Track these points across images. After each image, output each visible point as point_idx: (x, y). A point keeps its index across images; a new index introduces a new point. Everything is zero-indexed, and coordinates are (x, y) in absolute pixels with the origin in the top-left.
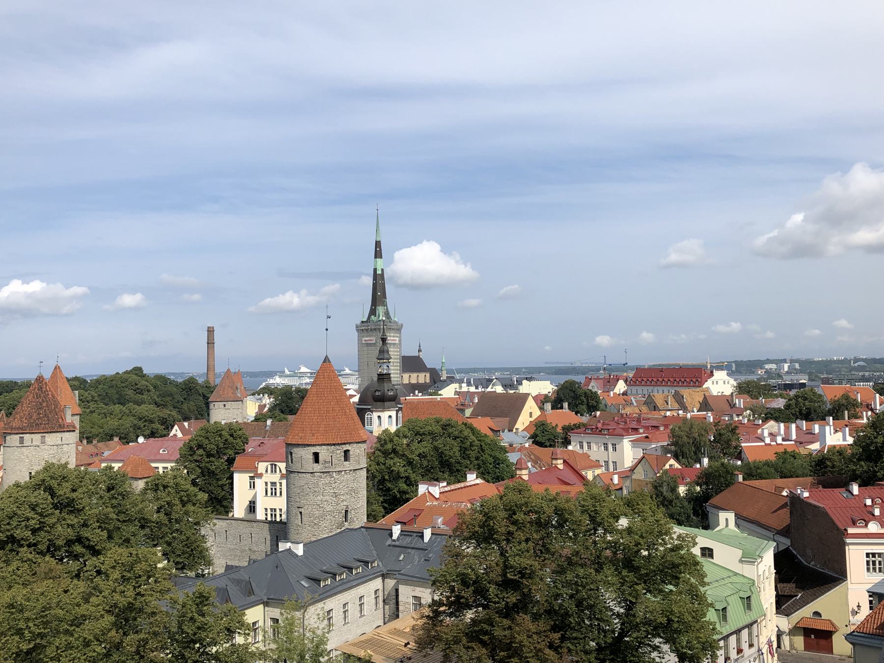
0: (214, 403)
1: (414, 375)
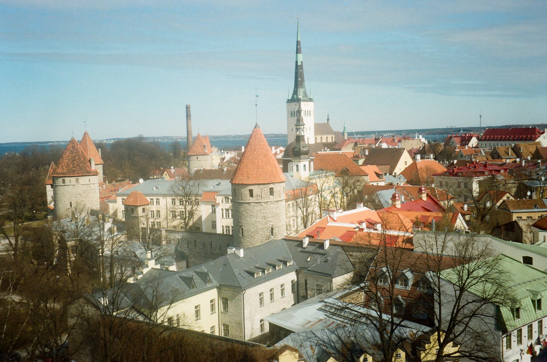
1: (324, 137)
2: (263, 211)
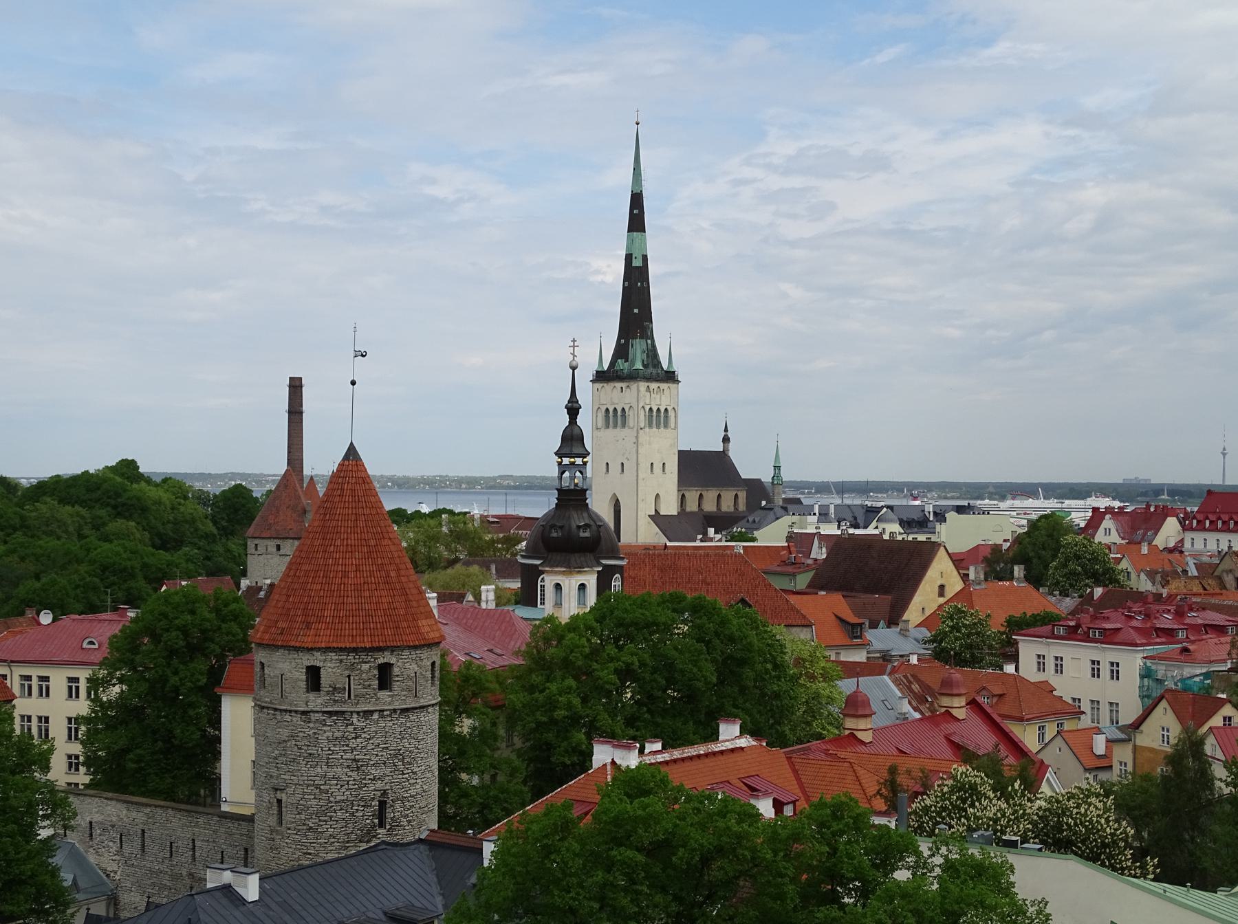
0: (257, 541)
1: (710, 495)
2: (353, 743)
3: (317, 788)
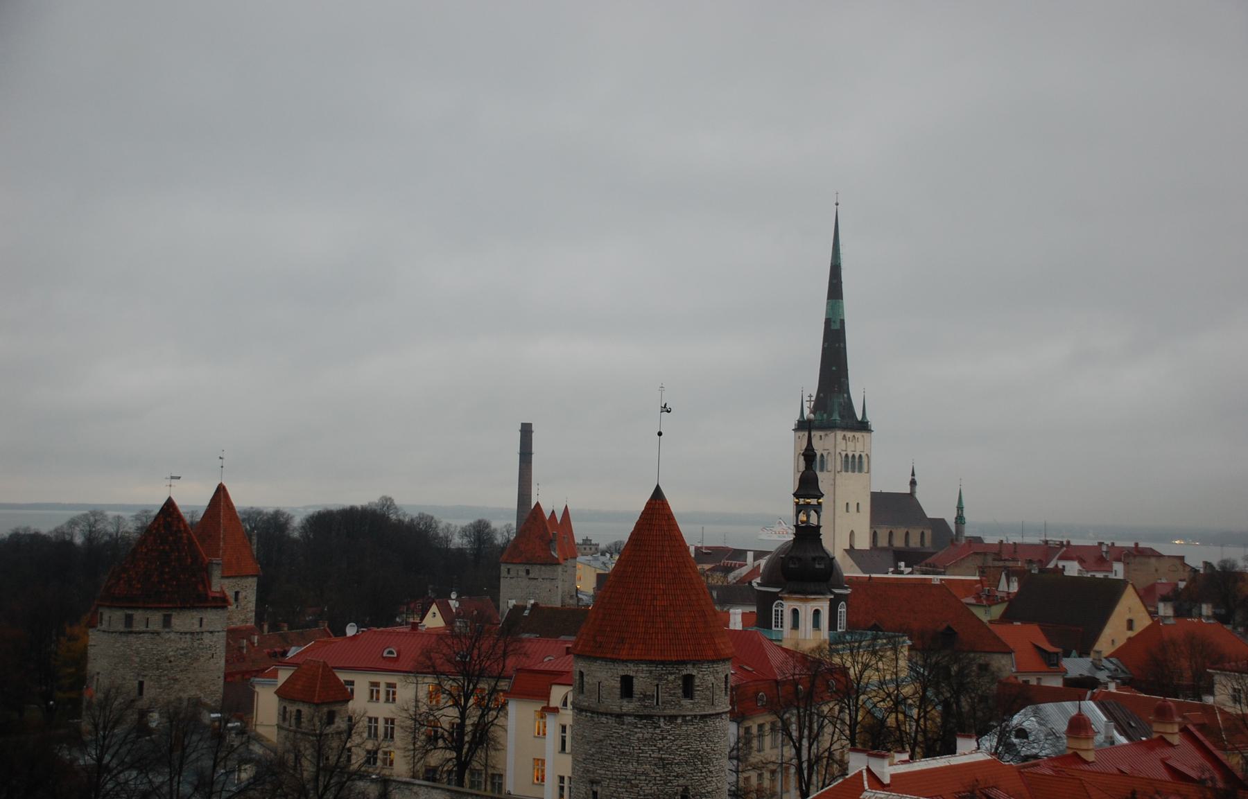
0: (509, 566)
3: (628, 782)
